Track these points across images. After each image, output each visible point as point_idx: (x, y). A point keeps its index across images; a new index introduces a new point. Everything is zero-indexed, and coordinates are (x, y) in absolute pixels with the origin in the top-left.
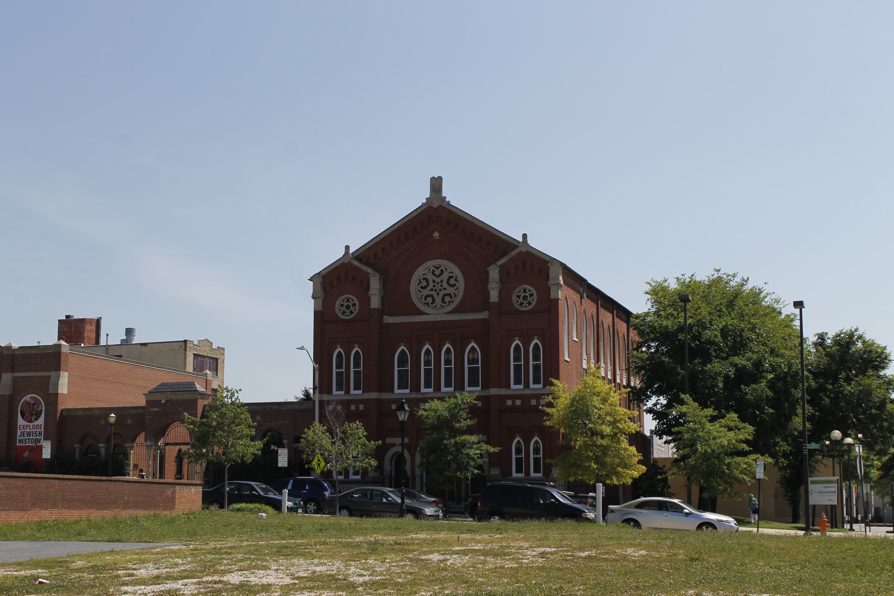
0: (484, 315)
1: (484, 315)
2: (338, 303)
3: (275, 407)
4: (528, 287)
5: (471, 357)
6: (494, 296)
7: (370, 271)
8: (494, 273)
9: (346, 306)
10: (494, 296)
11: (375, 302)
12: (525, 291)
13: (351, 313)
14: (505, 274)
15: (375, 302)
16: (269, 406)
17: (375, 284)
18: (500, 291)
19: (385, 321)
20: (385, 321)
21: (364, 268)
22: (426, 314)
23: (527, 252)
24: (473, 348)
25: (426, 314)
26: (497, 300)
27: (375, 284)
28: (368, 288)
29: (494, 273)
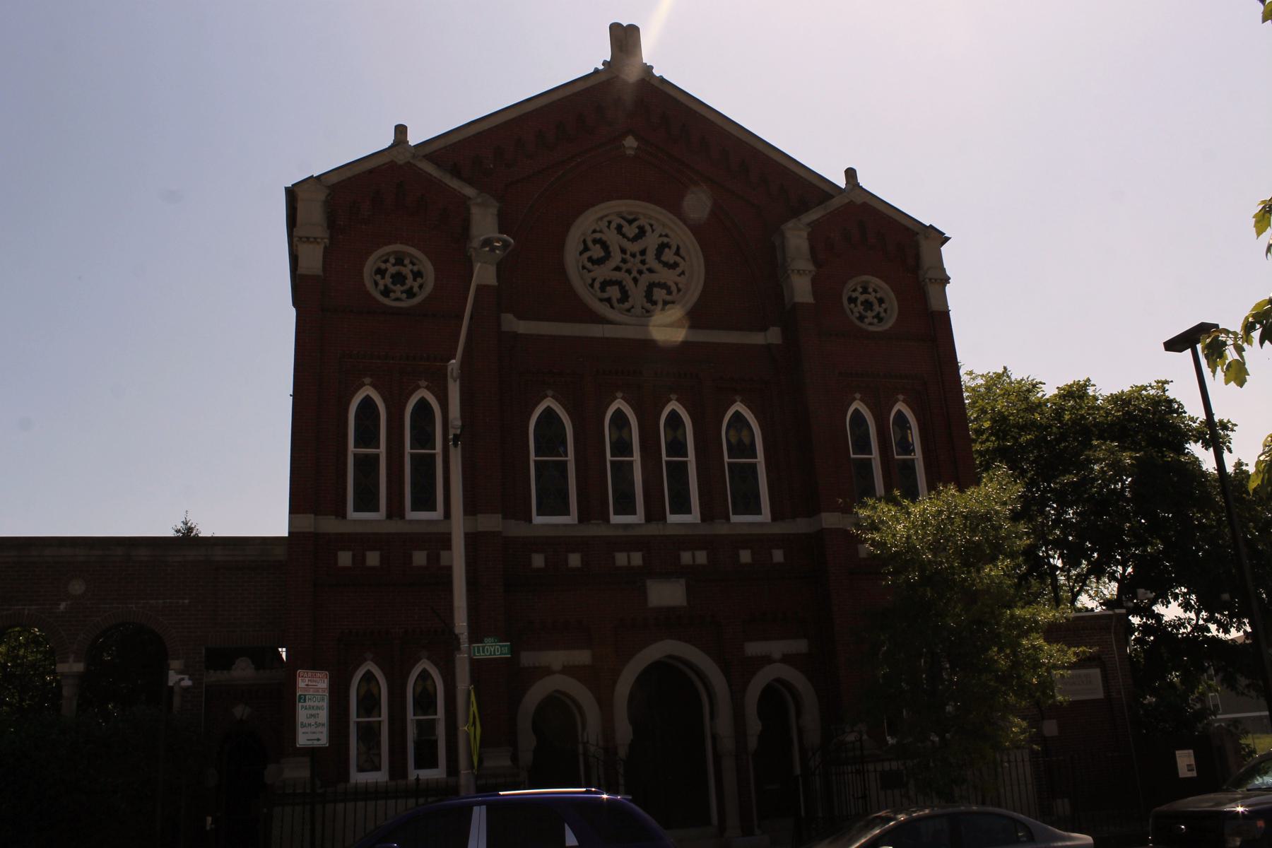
0: (773, 336)
1: (773, 336)
4: (875, 281)
6: (801, 288)
7: (469, 191)
8: (796, 238)
9: (399, 270)
10: (801, 288)
11: (484, 273)
12: (865, 291)
13: (410, 293)
14: (821, 249)
17: (484, 223)
18: (814, 282)
19: (505, 328)
20: (505, 328)
21: (455, 184)
23: (865, 204)
24: (738, 416)
26: (810, 300)
27: (484, 223)
29: (796, 238)
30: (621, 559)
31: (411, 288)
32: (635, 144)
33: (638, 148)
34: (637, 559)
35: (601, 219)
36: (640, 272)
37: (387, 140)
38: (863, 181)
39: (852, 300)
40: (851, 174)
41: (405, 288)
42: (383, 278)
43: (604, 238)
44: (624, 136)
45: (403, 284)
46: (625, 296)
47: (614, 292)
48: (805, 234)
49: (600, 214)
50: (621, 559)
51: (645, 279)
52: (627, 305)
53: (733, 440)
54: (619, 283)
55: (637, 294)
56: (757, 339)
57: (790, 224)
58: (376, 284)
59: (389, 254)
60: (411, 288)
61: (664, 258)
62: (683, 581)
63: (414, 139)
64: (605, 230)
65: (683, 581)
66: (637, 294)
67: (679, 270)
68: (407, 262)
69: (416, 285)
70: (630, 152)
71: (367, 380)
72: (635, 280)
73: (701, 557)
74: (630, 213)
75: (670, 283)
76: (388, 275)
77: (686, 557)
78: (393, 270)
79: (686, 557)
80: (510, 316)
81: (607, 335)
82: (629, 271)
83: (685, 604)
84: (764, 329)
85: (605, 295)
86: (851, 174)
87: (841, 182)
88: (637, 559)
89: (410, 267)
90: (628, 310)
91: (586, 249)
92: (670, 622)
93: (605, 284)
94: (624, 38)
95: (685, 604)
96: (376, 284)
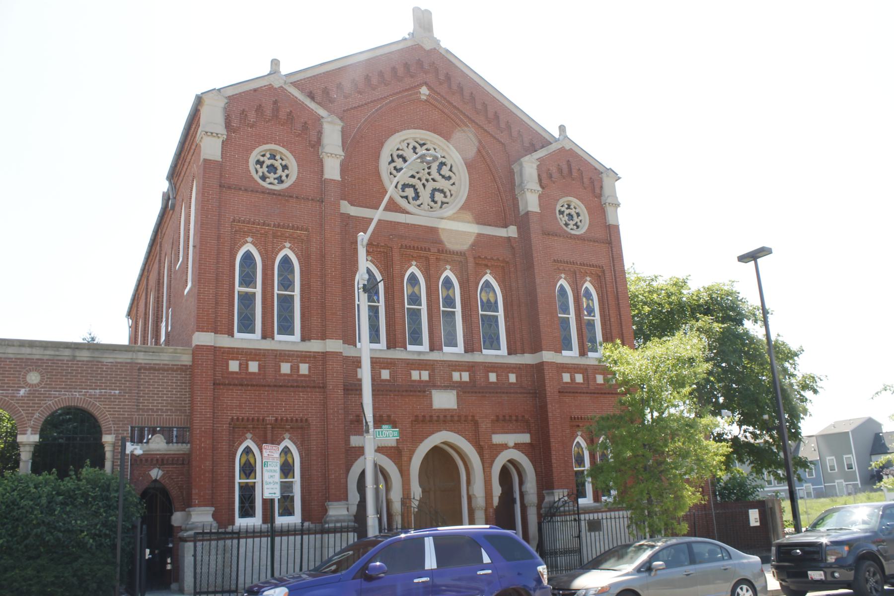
0: (512, 232)
1: (512, 232)
2: (254, 156)
3: (84, 355)
4: (575, 202)
5: (485, 300)
7: (322, 112)
8: (529, 168)
9: (274, 164)
10: (531, 202)
11: (332, 170)
12: (569, 207)
15: (332, 170)
16: (67, 352)
21: (312, 105)
22: (408, 213)
25: (408, 213)
26: (537, 210)
28: (318, 143)
29: (529, 168)
30: (415, 375)
31: (281, 177)
32: (427, 92)
33: (429, 95)
34: (425, 375)
35: (404, 141)
36: (427, 180)
37: (266, 70)
38: (570, 134)
39: (561, 213)
40: (562, 129)
41: (276, 176)
42: (261, 167)
43: (405, 155)
44: (420, 85)
45: (275, 173)
46: (417, 196)
47: (410, 192)
48: (535, 166)
49: (403, 138)
50: (415, 375)
51: (431, 185)
52: (418, 202)
53: (485, 300)
54: (413, 186)
55: (425, 195)
56: (502, 232)
57: (527, 158)
58: (257, 172)
59: (266, 151)
60: (281, 177)
61: (442, 172)
62: (455, 392)
63: (285, 70)
64: (405, 148)
65: (455, 392)
66: (425, 195)
67: (451, 182)
68: (278, 157)
69: (284, 175)
70: (424, 97)
71: (249, 239)
72: (424, 185)
73: (466, 377)
74: (422, 139)
75: (445, 190)
76: (265, 166)
77: (456, 376)
78: (268, 162)
79: (456, 376)
80: (346, 202)
81: (408, 222)
82: (420, 179)
83: (456, 407)
84: (506, 226)
85: (404, 194)
86: (562, 129)
87: (556, 134)
88: (425, 375)
89: (280, 161)
90: (419, 206)
91: (393, 161)
92: (445, 420)
93: (405, 186)
94: (423, 20)
95: (456, 407)
96: (257, 172)
